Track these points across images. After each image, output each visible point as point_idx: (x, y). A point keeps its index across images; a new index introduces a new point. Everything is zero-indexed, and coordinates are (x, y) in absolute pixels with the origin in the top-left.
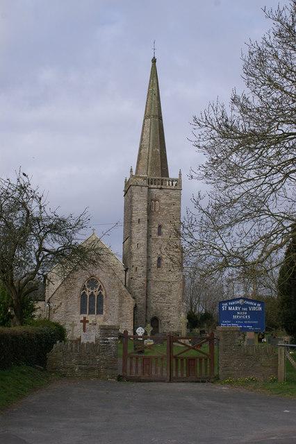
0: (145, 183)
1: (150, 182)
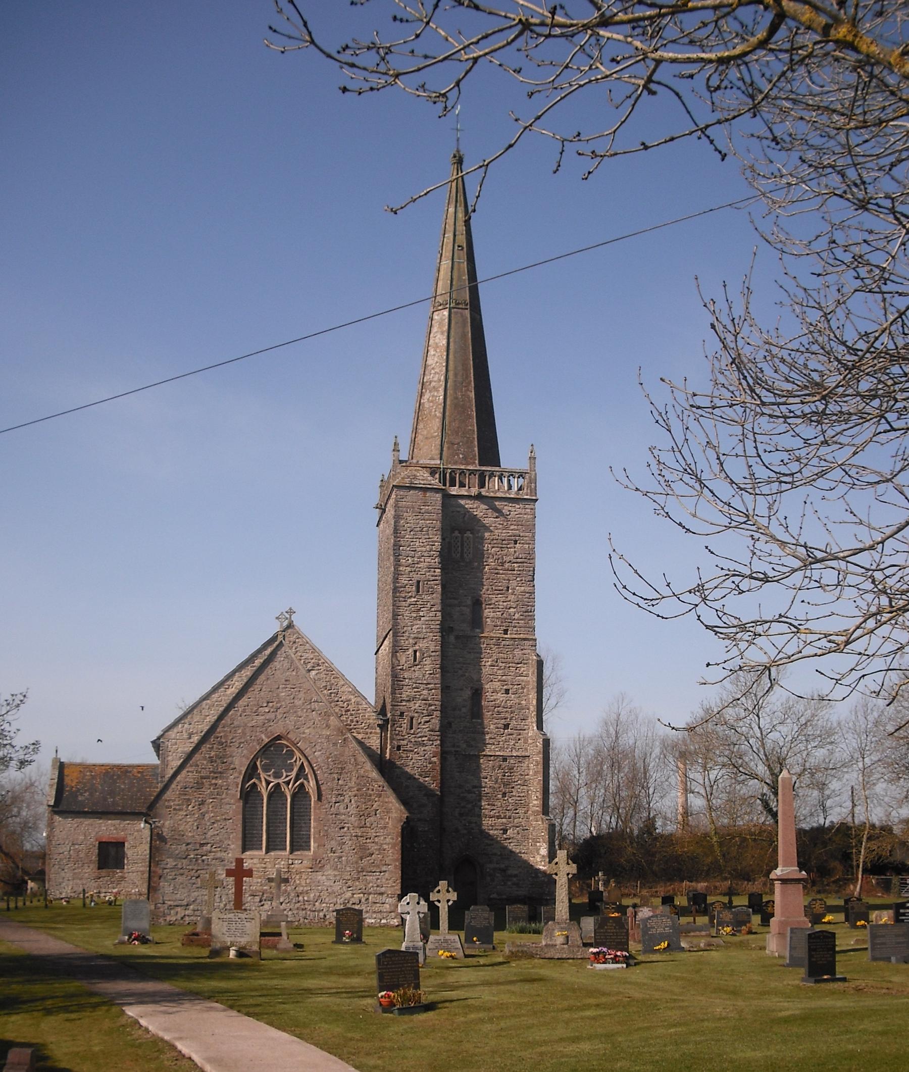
0: (435, 482)
1: (449, 478)
